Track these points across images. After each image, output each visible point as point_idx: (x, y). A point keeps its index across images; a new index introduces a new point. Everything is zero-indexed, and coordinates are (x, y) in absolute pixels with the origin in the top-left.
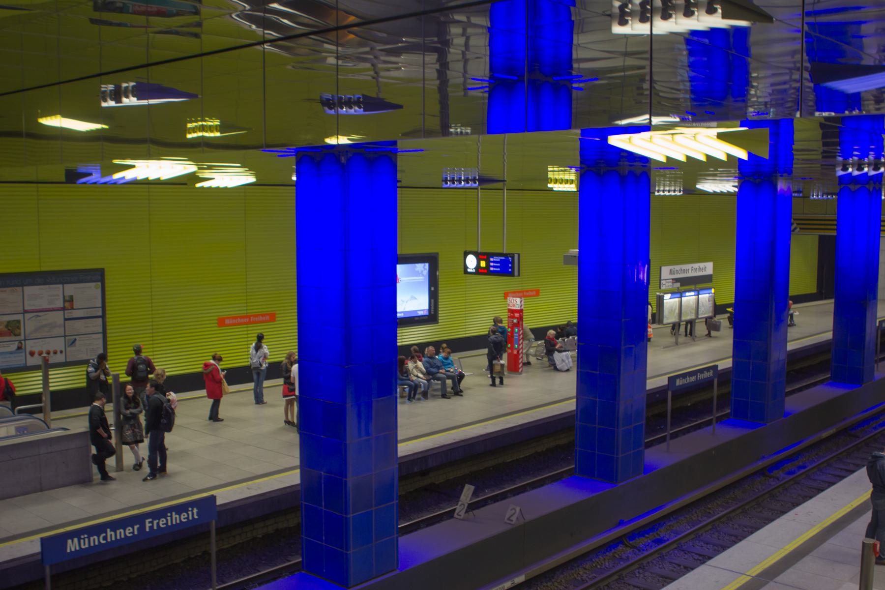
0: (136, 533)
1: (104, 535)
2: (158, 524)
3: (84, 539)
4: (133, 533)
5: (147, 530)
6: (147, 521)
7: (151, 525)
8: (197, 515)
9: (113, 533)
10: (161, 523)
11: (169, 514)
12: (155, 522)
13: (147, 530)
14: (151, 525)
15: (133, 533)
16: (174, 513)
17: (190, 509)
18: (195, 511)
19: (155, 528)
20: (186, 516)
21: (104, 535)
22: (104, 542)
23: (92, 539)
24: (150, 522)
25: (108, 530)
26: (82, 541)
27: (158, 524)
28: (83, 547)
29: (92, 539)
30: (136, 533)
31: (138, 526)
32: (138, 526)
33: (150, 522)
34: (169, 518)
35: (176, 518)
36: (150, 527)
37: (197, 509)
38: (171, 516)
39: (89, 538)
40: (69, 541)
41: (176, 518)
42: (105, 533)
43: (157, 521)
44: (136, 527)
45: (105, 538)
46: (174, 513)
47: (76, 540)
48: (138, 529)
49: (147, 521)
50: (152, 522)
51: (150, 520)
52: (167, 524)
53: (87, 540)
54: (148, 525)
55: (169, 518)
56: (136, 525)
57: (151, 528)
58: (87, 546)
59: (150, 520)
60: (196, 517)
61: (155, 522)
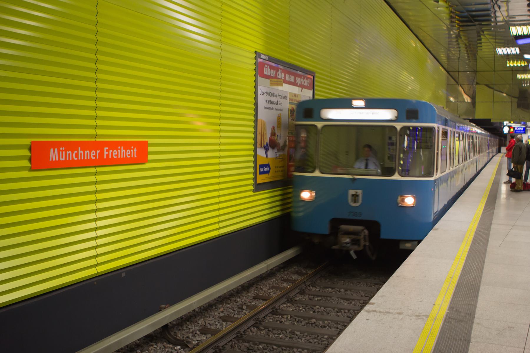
0: (97, 158)
1: (76, 152)
2: (112, 153)
3: (62, 151)
4: (95, 156)
5: (105, 157)
6: (106, 148)
7: (107, 153)
8: (136, 155)
10: (114, 154)
11: (119, 148)
12: (111, 151)
13: (105, 157)
14: (107, 153)
15: (95, 156)
16: (122, 147)
18: (135, 150)
19: (110, 157)
21: (76, 152)
22: (76, 159)
23: (68, 153)
24: (107, 151)
25: (79, 148)
26: (61, 152)
27: (112, 153)
28: (61, 159)
30: (97, 158)
33: (107, 151)
34: (119, 151)
35: (123, 152)
36: (107, 155)
37: (136, 149)
38: (120, 149)
40: (52, 150)
42: (76, 150)
43: (112, 151)
44: (98, 152)
45: (77, 155)
46: (122, 147)
47: (56, 150)
48: (99, 153)
49: (106, 148)
50: (107, 151)
51: (107, 148)
53: (64, 152)
54: (106, 153)
55: (119, 151)
56: (98, 150)
57: (108, 155)
59: (107, 148)
60: (135, 156)
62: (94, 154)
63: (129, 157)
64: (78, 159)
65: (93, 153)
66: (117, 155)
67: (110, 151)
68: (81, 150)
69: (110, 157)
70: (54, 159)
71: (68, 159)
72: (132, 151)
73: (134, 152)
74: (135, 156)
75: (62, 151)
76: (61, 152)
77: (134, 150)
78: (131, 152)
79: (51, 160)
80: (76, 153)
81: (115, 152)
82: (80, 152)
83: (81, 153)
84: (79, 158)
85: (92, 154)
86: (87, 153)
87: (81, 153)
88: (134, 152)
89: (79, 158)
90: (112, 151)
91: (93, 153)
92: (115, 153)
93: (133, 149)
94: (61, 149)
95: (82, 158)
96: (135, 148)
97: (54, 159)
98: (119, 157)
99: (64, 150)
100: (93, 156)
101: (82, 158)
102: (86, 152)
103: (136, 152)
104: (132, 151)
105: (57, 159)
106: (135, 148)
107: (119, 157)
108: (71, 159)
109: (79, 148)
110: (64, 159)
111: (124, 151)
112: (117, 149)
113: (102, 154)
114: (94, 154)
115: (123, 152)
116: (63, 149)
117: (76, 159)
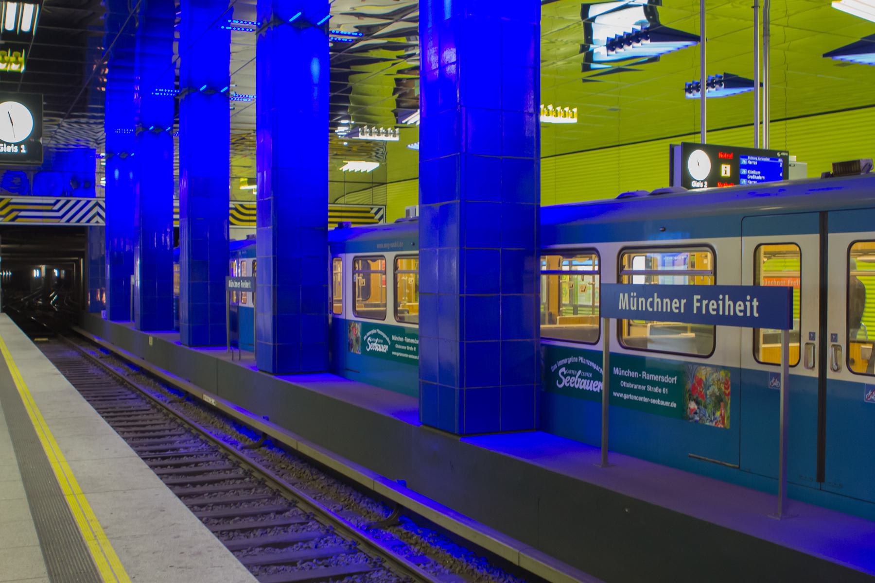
0: (682, 311)
1: (651, 299)
2: (707, 306)
4: (679, 308)
5: (695, 311)
7: (699, 304)
8: (757, 312)
9: (659, 300)
10: (711, 307)
11: (721, 297)
12: (705, 302)
13: (695, 311)
14: (699, 304)
15: (679, 308)
16: (727, 297)
17: (748, 298)
18: (755, 303)
19: (704, 312)
20: (742, 308)
21: (651, 299)
22: (651, 310)
23: (640, 300)
24: (698, 301)
25: (656, 295)
26: (632, 299)
27: (707, 306)
28: (632, 308)
29: (640, 300)
30: (682, 311)
31: (685, 301)
32: (685, 301)
33: (698, 301)
34: (721, 302)
35: (729, 306)
36: (697, 307)
37: (757, 301)
38: (724, 300)
39: (638, 297)
40: (621, 295)
43: (707, 301)
44: (683, 301)
46: (727, 297)
47: (626, 295)
48: (685, 304)
49: (696, 297)
51: (699, 297)
52: (717, 310)
53: (635, 299)
54: (696, 304)
55: (721, 302)
57: (699, 309)
58: (635, 308)
59: (699, 297)
60: (756, 315)
61: (705, 302)
62: (678, 305)
63: (677, 311)
64: (653, 309)
65: (676, 303)
66: (717, 310)
67: (704, 301)
68: (657, 298)
69: (704, 312)
70: (624, 308)
71: (640, 309)
72: (748, 304)
73: (752, 307)
74: (756, 315)
75: (633, 297)
76: (632, 299)
77: (753, 303)
78: (718, 305)
79: (620, 308)
80: (651, 302)
81: (713, 304)
82: (656, 300)
83: (658, 303)
84: (655, 310)
86: (667, 303)
87: (658, 303)
88: (752, 307)
89: (655, 310)
90: (707, 301)
91: (676, 303)
92: (713, 305)
93: (751, 301)
94: (632, 294)
95: (660, 310)
96: (755, 300)
97: (624, 308)
98: (721, 313)
99: (635, 297)
100: (676, 308)
101: (660, 310)
102: (665, 301)
103: (758, 307)
104: (748, 304)
105: (627, 308)
106: (755, 300)
107: (721, 313)
108: (669, 310)
109: (656, 295)
110: (635, 308)
111: (731, 303)
112: (717, 300)
113: (688, 306)
114: (678, 305)
115: (729, 306)
116: (635, 294)
117: (651, 310)
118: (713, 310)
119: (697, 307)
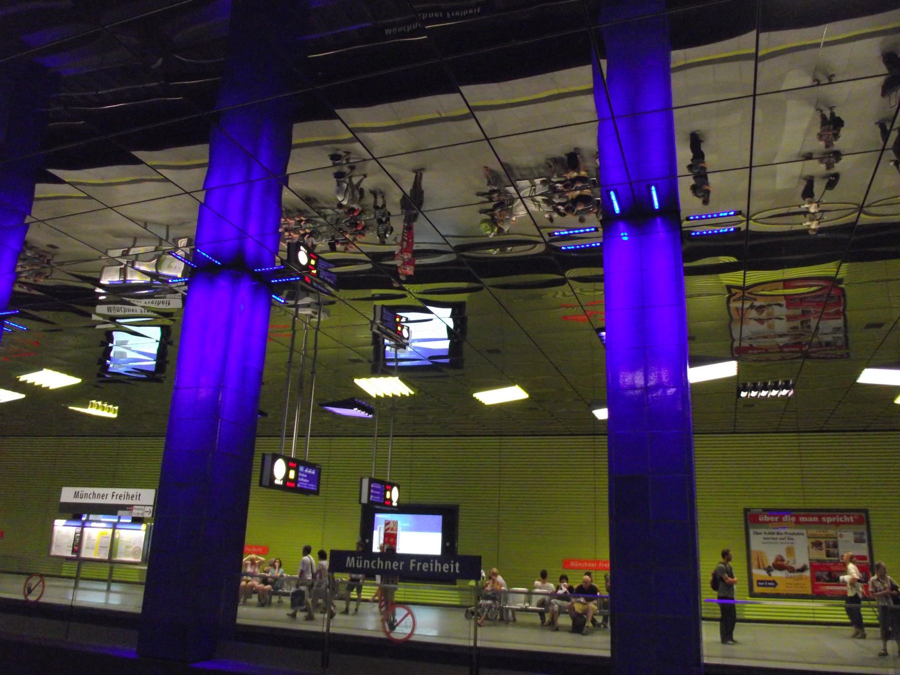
0: (401, 568)
2: (421, 566)
4: (399, 567)
7: (414, 565)
10: (424, 567)
12: (419, 564)
14: (414, 565)
17: (452, 562)
18: (457, 565)
20: (448, 567)
27: (421, 566)
30: (401, 568)
34: (432, 564)
35: (438, 566)
38: (434, 563)
41: (438, 566)
54: (412, 565)
55: (432, 564)
57: (415, 568)
72: (452, 565)
73: (455, 568)
85: (444, 568)
88: (455, 568)
93: (454, 564)
104: (452, 565)
118: (426, 568)
119: (413, 567)
